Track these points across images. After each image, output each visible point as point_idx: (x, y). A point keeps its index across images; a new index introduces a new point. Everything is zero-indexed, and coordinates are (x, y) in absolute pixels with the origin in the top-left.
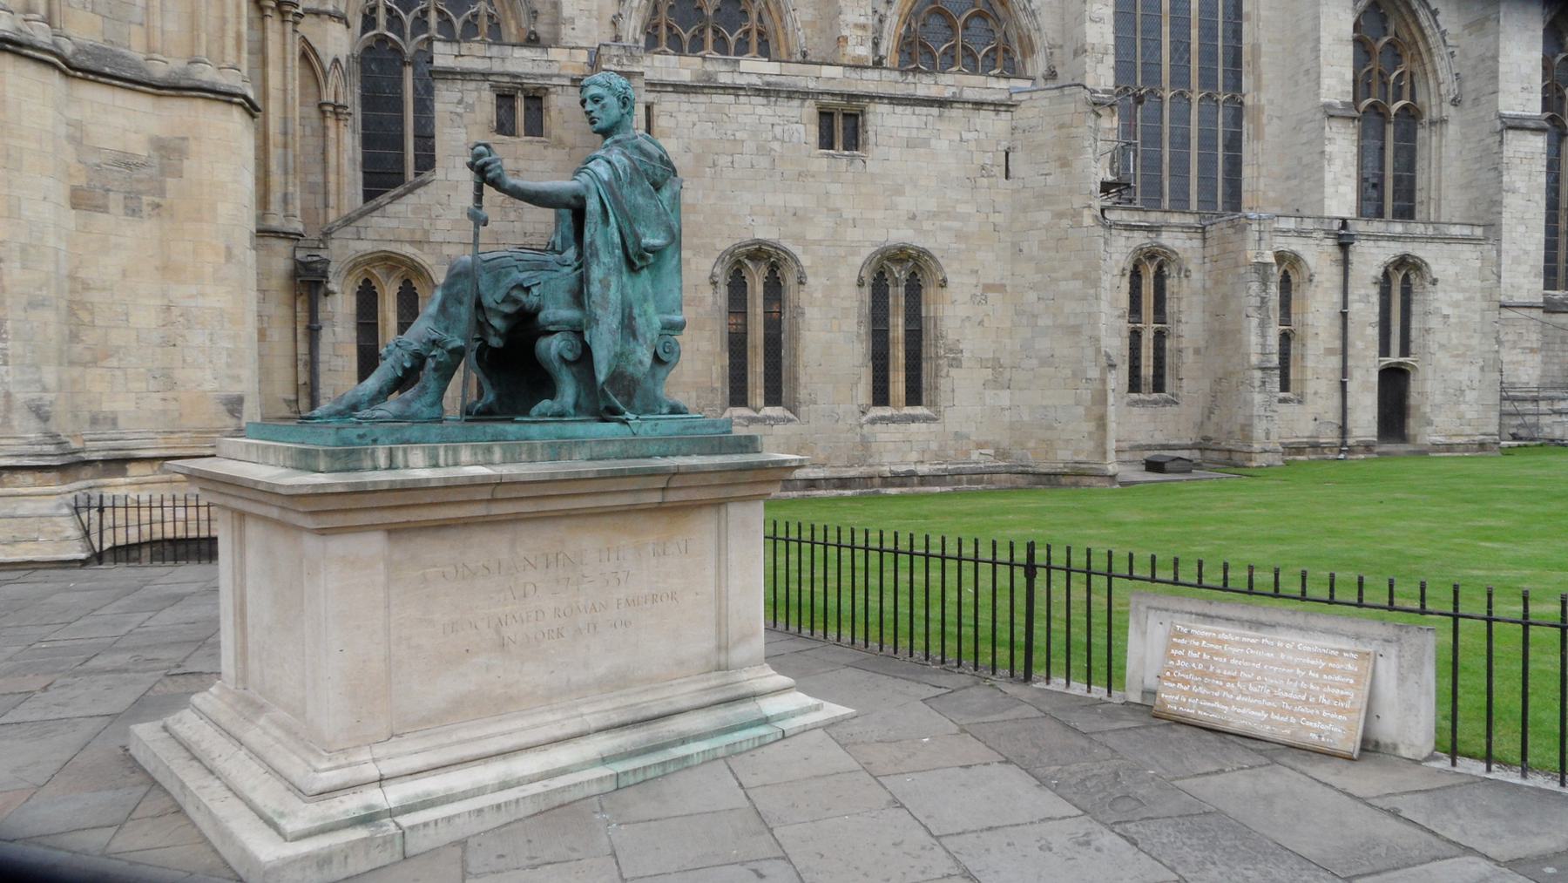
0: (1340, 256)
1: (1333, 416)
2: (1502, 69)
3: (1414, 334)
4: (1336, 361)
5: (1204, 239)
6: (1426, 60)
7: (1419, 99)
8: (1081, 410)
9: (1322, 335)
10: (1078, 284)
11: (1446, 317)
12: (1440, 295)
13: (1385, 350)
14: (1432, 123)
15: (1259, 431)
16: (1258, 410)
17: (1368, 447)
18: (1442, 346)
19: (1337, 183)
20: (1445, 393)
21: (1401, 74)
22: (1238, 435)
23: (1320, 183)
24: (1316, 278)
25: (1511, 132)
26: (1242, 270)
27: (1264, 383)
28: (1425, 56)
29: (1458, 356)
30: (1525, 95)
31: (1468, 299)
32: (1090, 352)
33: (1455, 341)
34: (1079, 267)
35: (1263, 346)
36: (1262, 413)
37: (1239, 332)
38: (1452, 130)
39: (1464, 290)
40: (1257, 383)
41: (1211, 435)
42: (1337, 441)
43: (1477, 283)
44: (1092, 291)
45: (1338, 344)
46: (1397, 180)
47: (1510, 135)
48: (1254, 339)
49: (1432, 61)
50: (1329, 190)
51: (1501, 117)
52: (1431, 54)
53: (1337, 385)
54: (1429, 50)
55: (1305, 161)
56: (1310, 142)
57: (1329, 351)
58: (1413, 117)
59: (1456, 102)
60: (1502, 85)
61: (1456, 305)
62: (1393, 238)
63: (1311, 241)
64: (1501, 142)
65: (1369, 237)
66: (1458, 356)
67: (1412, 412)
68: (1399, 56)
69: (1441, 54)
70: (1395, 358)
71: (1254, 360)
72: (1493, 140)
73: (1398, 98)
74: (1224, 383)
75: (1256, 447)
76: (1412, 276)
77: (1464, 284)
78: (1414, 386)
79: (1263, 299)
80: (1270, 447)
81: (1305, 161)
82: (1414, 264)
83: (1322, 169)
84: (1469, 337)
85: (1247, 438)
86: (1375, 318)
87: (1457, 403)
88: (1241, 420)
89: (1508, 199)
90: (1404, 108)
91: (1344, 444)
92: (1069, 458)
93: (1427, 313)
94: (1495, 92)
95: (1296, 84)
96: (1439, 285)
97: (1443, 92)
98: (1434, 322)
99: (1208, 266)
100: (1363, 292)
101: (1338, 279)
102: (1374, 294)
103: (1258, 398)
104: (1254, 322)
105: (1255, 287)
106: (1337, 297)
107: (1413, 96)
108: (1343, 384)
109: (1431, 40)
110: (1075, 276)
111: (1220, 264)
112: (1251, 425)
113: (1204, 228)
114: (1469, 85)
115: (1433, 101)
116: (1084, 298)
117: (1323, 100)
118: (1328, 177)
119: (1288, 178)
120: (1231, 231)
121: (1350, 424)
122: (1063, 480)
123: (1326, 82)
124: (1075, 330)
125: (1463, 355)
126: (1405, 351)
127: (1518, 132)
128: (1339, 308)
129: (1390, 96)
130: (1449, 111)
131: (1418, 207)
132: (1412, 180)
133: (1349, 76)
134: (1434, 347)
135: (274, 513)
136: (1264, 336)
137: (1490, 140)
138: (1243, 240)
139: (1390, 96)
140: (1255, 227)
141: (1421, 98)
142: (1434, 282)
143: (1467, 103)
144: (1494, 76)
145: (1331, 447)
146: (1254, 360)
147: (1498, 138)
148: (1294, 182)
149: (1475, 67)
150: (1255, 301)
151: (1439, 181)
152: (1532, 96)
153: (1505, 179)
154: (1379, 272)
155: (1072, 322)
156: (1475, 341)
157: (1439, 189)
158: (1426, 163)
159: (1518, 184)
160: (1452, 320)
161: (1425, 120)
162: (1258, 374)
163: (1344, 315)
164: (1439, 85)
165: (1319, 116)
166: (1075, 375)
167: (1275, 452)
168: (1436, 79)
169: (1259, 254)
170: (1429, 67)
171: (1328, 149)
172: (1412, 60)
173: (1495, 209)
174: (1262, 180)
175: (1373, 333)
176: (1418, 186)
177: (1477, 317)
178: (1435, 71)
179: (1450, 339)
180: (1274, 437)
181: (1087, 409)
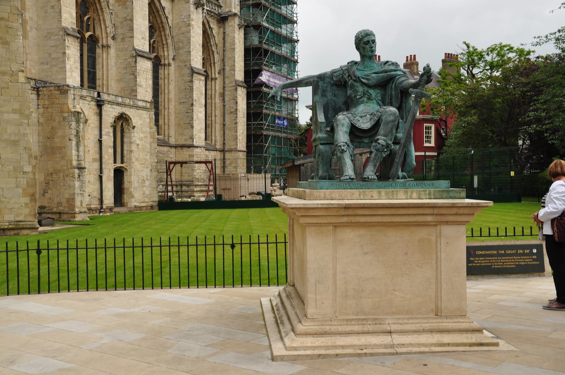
0: (98, 111)
1: (96, 194)
2: (135, 26)
3: (125, 152)
4: (96, 165)
5: (38, 95)
6: (100, 14)
7: (97, 33)
8: (20, 190)
9: (91, 152)
10: (16, 116)
11: (138, 145)
12: (136, 134)
13: (115, 162)
14: (103, 46)
15: (78, 203)
16: (77, 191)
17: (111, 209)
18: (137, 159)
19: (72, 71)
20: (138, 182)
21: (89, 18)
22: (65, 204)
23: (63, 69)
24: (89, 122)
25: (139, 58)
26: (66, 115)
27: (79, 176)
28: (100, 11)
29: (142, 164)
30: (143, 41)
31: (145, 137)
32: (26, 156)
33: (141, 157)
34: (17, 106)
35: (78, 156)
36: (79, 192)
37: (64, 148)
38: (112, 51)
39: (143, 132)
40: (76, 176)
41: (46, 205)
42: (99, 207)
43: (148, 129)
44: (26, 121)
45: (97, 156)
46: (89, 72)
47: (139, 59)
48: (74, 152)
49: (103, 15)
50: (68, 74)
51: (135, 50)
52: (102, 11)
53: (97, 177)
54: (102, 9)
55: (53, 56)
56: (56, 46)
57: (94, 160)
58: (94, 41)
59: (114, 38)
60: (135, 34)
61: (141, 139)
62: (118, 104)
63: (85, 102)
64: (136, 62)
65: (110, 102)
66: (142, 164)
67: (125, 191)
68: (87, 8)
69: (106, 11)
70: (119, 165)
71: (75, 163)
72: (132, 60)
73: (88, 31)
74: (54, 176)
75: (77, 210)
76: (124, 124)
77: (144, 130)
78: (126, 178)
79: (77, 131)
80: (83, 210)
81: (53, 56)
82: (126, 118)
83: (64, 62)
84: (146, 155)
85: (72, 206)
86: (112, 144)
87: (143, 187)
88: (67, 196)
89: (139, 90)
90: (90, 36)
91: (102, 208)
92: (13, 219)
93: (131, 143)
94: (132, 37)
95: (46, 12)
96: (135, 129)
97: (108, 31)
98: (134, 147)
99: (41, 110)
100: (107, 130)
101: (97, 123)
102: (111, 130)
103: (77, 184)
104: (74, 143)
105: (74, 124)
106: (97, 132)
107: (94, 32)
108: (101, 177)
109: (103, 4)
110: (14, 111)
111: (50, 110)
112: (73, 199)
113: (38, 88)
114: (120, 31)
115: (104, 35)
116: (21, 124)
117: (64, 25)
118: (68, 67)
119: (42, 63)
120: (57, 92)
121: (104, 198)
122: (8, 233)
123: (64, 16)
124: (15, 143)
125: (144, 164)
126: (122, 162)
127: (142, 58)
128: (98, 137)
129: (85, 29)
130: (111, 42)
131: (97, 87)
132: (94, 74)
133: (74, 15)
134: (134, 159)
135: (429, 218)
136: (78, 151)
137: (130, 60)
138: (67, 98)
139: (85, 29)
140: (72, 92)
141: (98, 33)
142: (134, 127)
143: (119, 40)
144: (131, 29)
145: (96, 210)
146: (75, 163)
147: (134, 59)
148: (46, 67)
149: (122, 23)
150: (74, 132)
151: (108, 77)
152: (146, 42)
153: (138, 80)
154: (112, 120)
155: (12, 138)
156: (148, 157)
157: (108, 80)
158: (101, 66)
159: (143, 83)
160: (140, 147)
161: (100, 44)
162: (77, 171)
163: (100, 142)
164: (106, 28)
165: (61, 33)
166: (15, 169)
167: (85, 212)
168: (105, 24)
169: (74, 107)
170: (101, 17)
171: (67, 52)
172: (94, 12)
173: (133, 94)
174: (28, 62)
175: (111, 151)
176: (97, 77)
177: (148, 146)
178: (104, 20)
179: (139, 156)
180: (84, 205)
181: (24, 190)
